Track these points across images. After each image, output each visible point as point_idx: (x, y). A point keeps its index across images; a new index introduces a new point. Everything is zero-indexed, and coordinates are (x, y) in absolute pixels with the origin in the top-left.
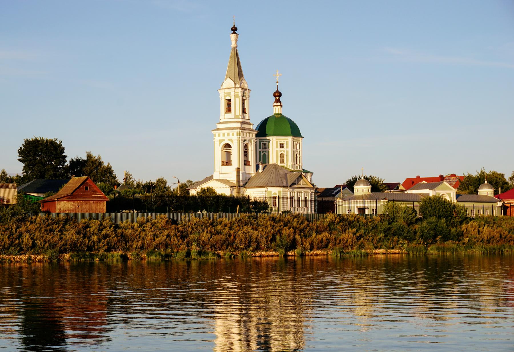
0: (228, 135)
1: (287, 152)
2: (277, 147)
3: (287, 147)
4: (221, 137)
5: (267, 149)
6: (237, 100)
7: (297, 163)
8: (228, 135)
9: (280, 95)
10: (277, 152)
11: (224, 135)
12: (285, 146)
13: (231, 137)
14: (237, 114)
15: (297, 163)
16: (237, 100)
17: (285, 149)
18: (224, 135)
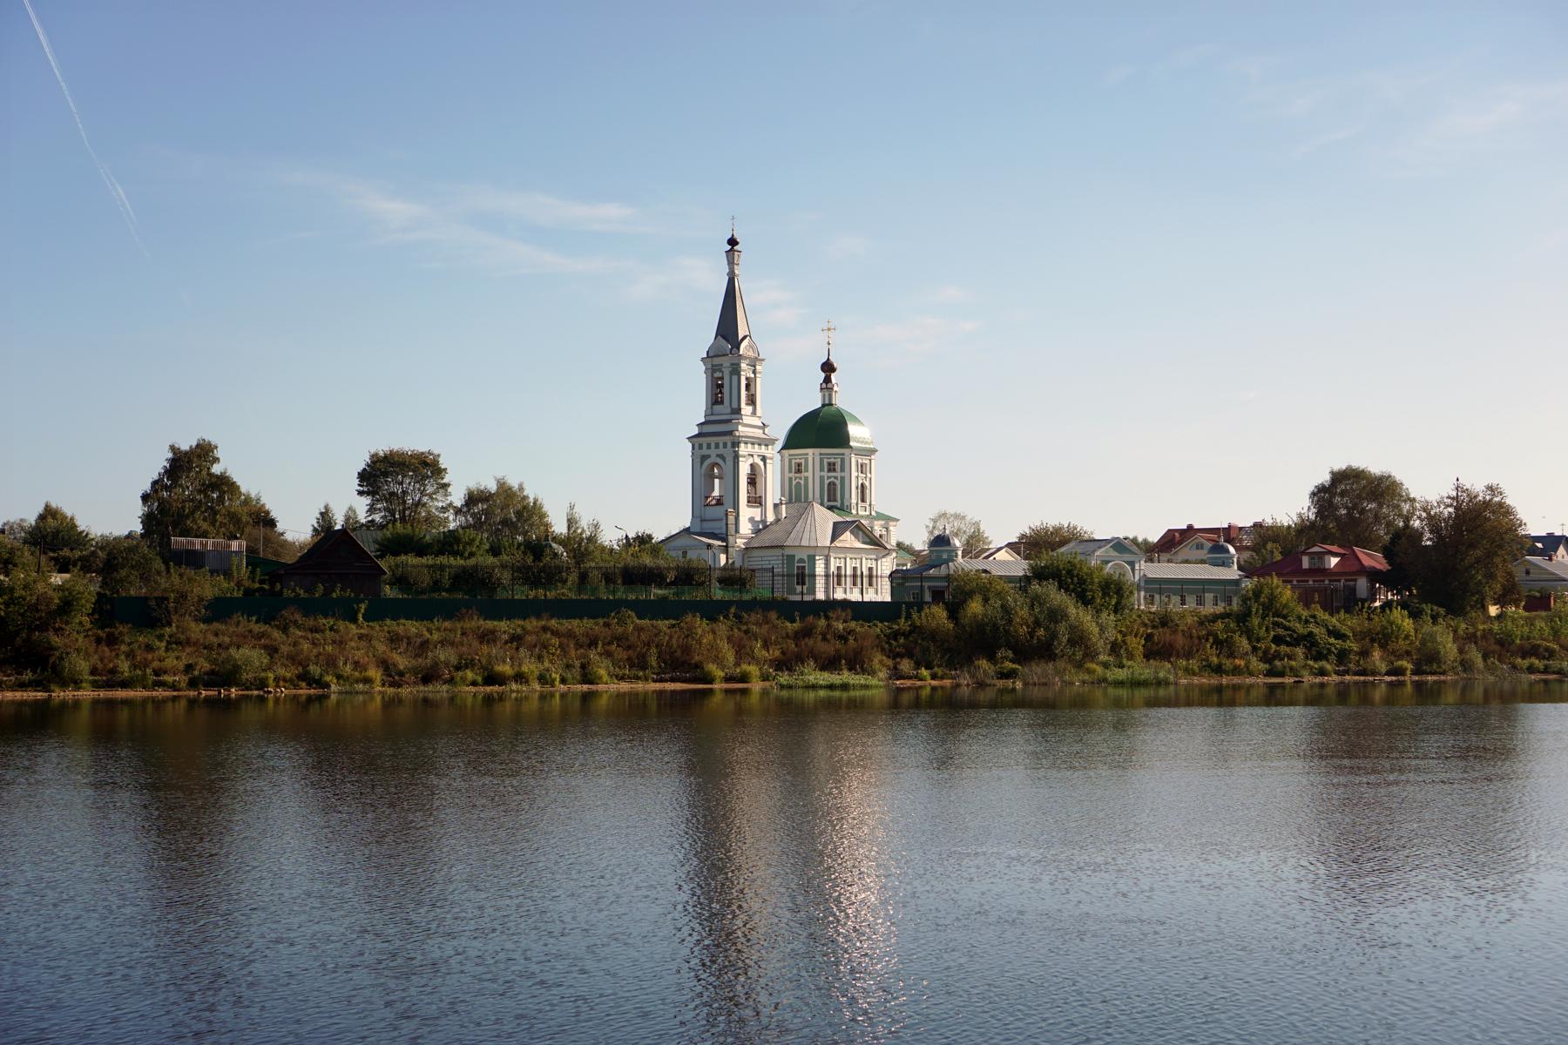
0: (717, 446)
1: (843, 479)
2: (822, 470)
3: (842, 470)
4: (705, 451)
5: (804, 474)
6: (735, 378)
7: (863, 500)
8: (717, 446)
9: (833, 370)
10: (822, 478)
11: (709, 446)
12: (838, 467)
13: (721, 450)
14: (735, 405)
15: (863, 500)
16: (735, 378)
17: (838, 474)
18: (709, 446)
